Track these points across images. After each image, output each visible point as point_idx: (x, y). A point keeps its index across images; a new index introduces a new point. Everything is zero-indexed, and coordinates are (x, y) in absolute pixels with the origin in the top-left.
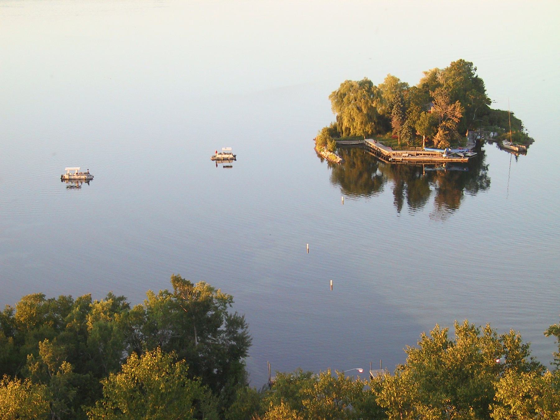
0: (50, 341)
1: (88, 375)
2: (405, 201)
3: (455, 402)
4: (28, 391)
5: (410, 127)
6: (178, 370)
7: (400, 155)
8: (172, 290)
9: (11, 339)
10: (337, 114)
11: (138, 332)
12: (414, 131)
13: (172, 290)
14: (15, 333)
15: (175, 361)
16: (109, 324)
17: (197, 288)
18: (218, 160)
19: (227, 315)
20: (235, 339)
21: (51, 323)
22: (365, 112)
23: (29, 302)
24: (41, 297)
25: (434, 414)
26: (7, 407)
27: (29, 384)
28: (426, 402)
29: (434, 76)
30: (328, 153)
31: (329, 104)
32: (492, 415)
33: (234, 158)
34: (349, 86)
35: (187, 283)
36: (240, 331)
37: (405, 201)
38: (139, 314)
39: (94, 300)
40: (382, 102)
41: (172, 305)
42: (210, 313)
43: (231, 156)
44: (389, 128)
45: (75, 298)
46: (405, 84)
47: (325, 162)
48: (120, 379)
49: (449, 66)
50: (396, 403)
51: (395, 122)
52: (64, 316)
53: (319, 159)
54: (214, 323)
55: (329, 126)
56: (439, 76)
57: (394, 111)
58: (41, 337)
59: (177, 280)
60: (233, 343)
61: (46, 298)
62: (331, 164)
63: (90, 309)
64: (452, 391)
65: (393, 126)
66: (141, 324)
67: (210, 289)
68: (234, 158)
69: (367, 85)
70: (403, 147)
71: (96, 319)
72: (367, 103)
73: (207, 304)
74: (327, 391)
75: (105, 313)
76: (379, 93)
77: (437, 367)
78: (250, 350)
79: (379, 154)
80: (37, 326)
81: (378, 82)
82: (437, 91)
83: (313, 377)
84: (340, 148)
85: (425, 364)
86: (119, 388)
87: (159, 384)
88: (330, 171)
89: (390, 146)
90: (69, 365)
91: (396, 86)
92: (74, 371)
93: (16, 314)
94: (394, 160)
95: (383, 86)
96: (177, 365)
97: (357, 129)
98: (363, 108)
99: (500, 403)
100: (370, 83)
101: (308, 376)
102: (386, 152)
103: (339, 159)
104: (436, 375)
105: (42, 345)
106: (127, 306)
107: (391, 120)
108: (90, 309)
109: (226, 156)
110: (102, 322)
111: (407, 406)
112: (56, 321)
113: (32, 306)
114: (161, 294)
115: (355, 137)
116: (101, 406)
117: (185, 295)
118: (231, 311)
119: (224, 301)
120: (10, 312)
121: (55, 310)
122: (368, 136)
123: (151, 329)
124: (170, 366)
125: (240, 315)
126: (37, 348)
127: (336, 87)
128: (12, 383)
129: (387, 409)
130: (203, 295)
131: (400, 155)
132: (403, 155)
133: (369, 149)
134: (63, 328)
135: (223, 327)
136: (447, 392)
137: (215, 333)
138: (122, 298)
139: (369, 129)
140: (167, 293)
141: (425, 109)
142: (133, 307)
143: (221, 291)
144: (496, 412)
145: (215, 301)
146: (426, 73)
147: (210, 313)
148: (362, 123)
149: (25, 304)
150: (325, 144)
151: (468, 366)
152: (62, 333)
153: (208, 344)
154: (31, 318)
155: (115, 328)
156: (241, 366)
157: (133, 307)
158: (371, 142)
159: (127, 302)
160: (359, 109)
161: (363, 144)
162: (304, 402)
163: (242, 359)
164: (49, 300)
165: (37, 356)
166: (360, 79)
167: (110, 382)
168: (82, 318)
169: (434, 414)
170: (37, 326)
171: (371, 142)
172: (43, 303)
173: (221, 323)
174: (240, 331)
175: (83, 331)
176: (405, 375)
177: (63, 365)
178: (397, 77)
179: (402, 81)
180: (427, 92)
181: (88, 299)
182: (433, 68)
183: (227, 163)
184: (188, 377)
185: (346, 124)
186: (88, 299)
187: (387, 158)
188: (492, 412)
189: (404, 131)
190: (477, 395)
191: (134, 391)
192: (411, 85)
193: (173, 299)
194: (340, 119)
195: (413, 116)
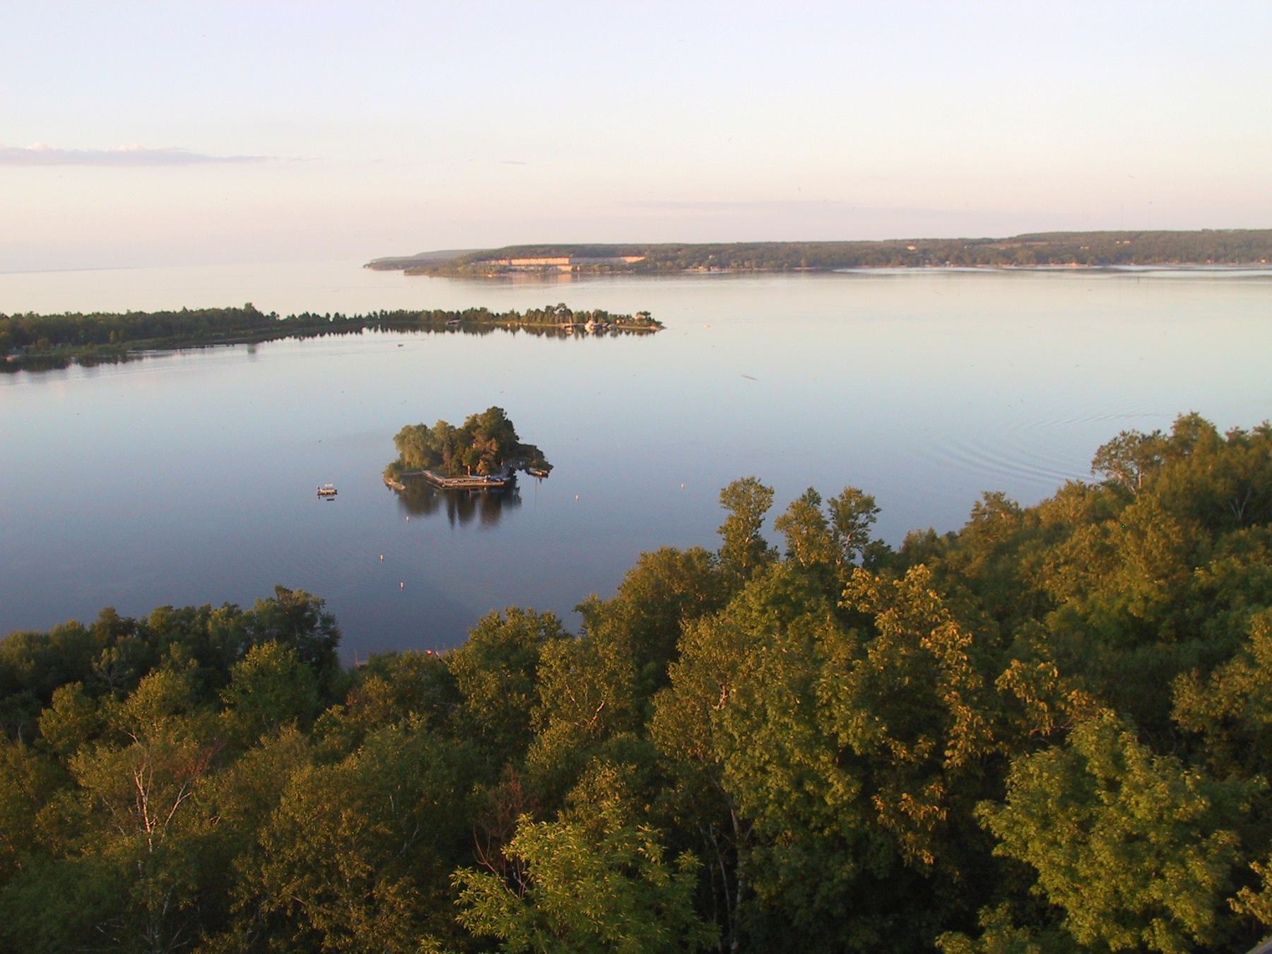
0: (179, 643)
1: (211, 668)
2: (457, 515)
3: (509, 667)
4: (171, 679)
5: (458, 460)
6: (291, 657)
7: (451, 482)
8: (275, 598)
9: (147, 643)
10: (400, 452)
11: (250, 632)
12: (461, 463)
13: (275, 598)
14: (150, 638)
15: (288, 650)
16: (226, 627)
17: (295, 594)
18: (323, 494)
19: (320, 614)
20: (328, 633)
21: (179, 628)
22: (422, 449)
23: (160, 612)
24: (170, 608)
25: (494, 677)
26: (156, 693)
27: (172, 674)
28: (486, 668)
29: (475, 418)
30: (394, 483)
31: (394, 444)
32: (538, 674)
33: (335, 493)
34: (408, 430)
35: (286, 591)
36: (332, 626)
37: (457, 515)
38: (250, 618)
39: (212, 609)
40: (435, 441)
41: (276, 609)
42: (307, 614)
43: (333, 491)
44: (441, 461)
45: (197, 609)
46: (452, 427)
47: (392, 490)
48: (244, 666)
49: (486, 412)
50: (465, 671)
51: (446, 455)
52: (189, 622)
53: (387, 488)
54: (311, 621)
55: (394, 462)
56: (478, 420)
57: (444, 448)
58: (171, 640)
59: (279, 589)
60: (327, 636)
61: (174, 609)
62: (397, 491)
63: (210, 616)
64: (506, 659)
65: (445, 459)
66: (251, 626)
67: (307, 595)
68: (335, 493)
69: (423, 428)
70: (453, 476)
71: (215, 623)
72: (423, 443)
73: (304, 607)
74: (410, 665)
75: (222, 618)
76: (432, 434)
77: (493, 641)
78: (340, 641)
79: (436, 482)
80: (168, 631)
81: (431, 425)
82: (477, 431)
83: (398, 655)
84: (403, 479)
85: (484, 640)
86: (245, 673)
87: (276, 667)
88: (397, 496)
89: (443, 475)
90: (195, 661)
91: (446, 429)
92: (200, 666)
93: (150, 622)
94: (446, 486)
95: (435, 429)
96: (290, 652)
97: (417, 461)
98: (420, 447)
99: (544, 664)
100: (425, 427)
101: (394, 655)
102: (440, 480)
103: (403, 487)
104: (493, 647)
105: (173, 647)
106: (240, 612)
107: (442, 455)
108: (210, 616)
109: (329, 491)
110: (220, 625)
111: (473, 672)
112: (183, 627)
113: (162, 616)
114: (267, 601)
115: (416, 470)
116: (231, 688)
117: (286, 601)
118: (324, 611)
119: (319, 603)
120: (145, 622)
121: (182, 618)
122: (425, 469)
123: (260, 629)
124: (285, 654)
125: (331, 614)
126: (168, 649)
127: (399, 431)
128: (158, 674)
129: (457, 676)
130: (301, 600)
131: (451, 482)
132: (454, 482)
133: (427, 478)
134: (189, 632)
135: (318, 624)
136: (502, 659)
137: (312, 629)
138: (235, 606)
139: (426, 463)
140: (272, 600)
141: (469, 445)
142: (244, 613)
143: (315, 595)
144: (541, 670)
145: (310, 604)
146: (468, 418)
147: (307, 614)
148: (420, 458)
149: (157, 614)
150: (391, 476)
151: (517, 639)
152: (189, 637)
153: (307, 639)
154: (162, 626)
155: (231, 630)
156: (334, 655)
157: (244, 613)
158: (428, 474)
159: (239, 608)
160: (418, 448)
161: (422, 475)
162: (393, 675)
163: (334, 649)
164: (177, 610)
165: (169, 655)
166: (418, 424)
167: (237, 669)
168: (204, 623)
169: (494, 677)
170: (168, 631)
171: (428, 474)
172: (171, 613)
173: (316, 621)
174: (332, 626)
175: (205, 634)
176: (471, 648)
177: (191, 662)
178: (446, 421)
179: (450, 425)
180: (469, 432)
181: (209, 608)
182: (473, 414)
183: (330, 497)
184: (299, 661)
185: (407, 459)
186: (209, 608)
187: (441, 485)
188: (538, 671)
189: (453, 463)
190: (525, 661)
191: (256, 675)
192: (457, 428)
193: (277, 604)
194: (402, 455)
195: (460, 451)
